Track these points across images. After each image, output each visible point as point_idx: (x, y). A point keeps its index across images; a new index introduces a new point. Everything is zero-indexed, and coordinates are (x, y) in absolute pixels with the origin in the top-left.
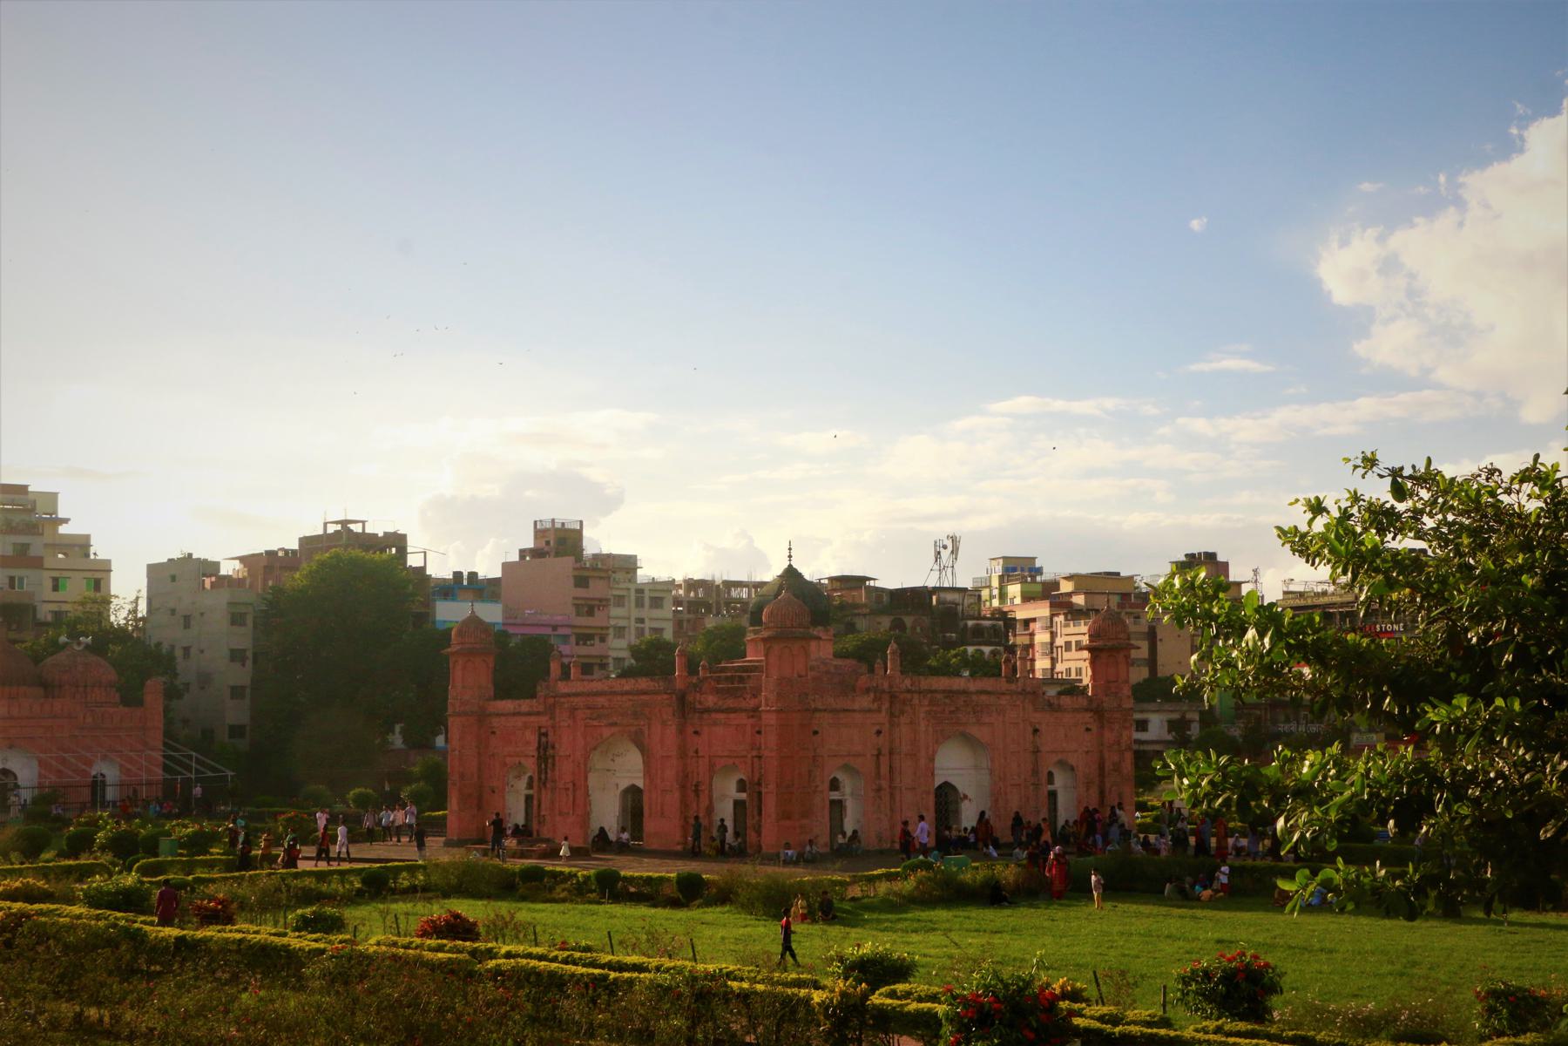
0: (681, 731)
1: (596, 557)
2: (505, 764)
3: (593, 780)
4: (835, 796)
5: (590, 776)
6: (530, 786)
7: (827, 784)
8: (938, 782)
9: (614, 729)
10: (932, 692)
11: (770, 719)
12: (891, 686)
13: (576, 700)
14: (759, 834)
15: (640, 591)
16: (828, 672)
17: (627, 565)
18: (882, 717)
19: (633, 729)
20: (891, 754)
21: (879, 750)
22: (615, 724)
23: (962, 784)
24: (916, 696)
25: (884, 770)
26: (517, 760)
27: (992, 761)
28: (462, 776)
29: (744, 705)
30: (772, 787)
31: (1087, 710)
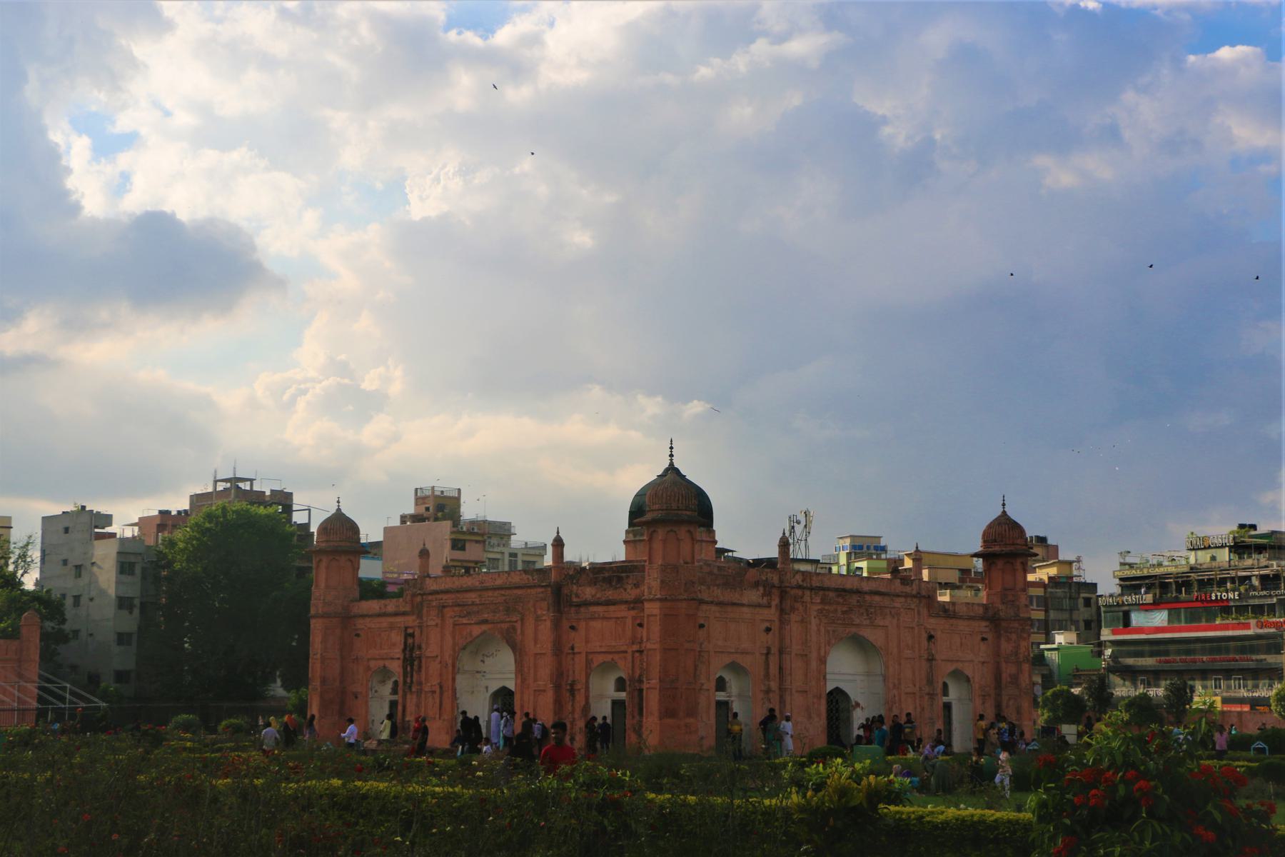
0: (557, 625)
1: (473, 522)
2: (369, 668)
3: (462, 682)
4: (721, 696)
5: (459, 678)
6: (394, 691)
7: (713, 684)
8: (830, 687)
9: (485, 627)
10: (822, 589)
11: (652, 609)
12: (781, 581)
13: (445, 597)
14: (640, 736)
15: (513, 555)
16: (711, 573)
17: (502, 531)
18: (772, 614)
19: (505, 626)
20: (781, 652)
21: (769, 649)
22: (485, 622)
23: (855, 692)
24: (808, 593)
25: (774, 670)
26: (381, 663)
27: (887, 667)
28: (324, 680)
29: (626, 597)
30: (655, 682)
31: (982, 618)
